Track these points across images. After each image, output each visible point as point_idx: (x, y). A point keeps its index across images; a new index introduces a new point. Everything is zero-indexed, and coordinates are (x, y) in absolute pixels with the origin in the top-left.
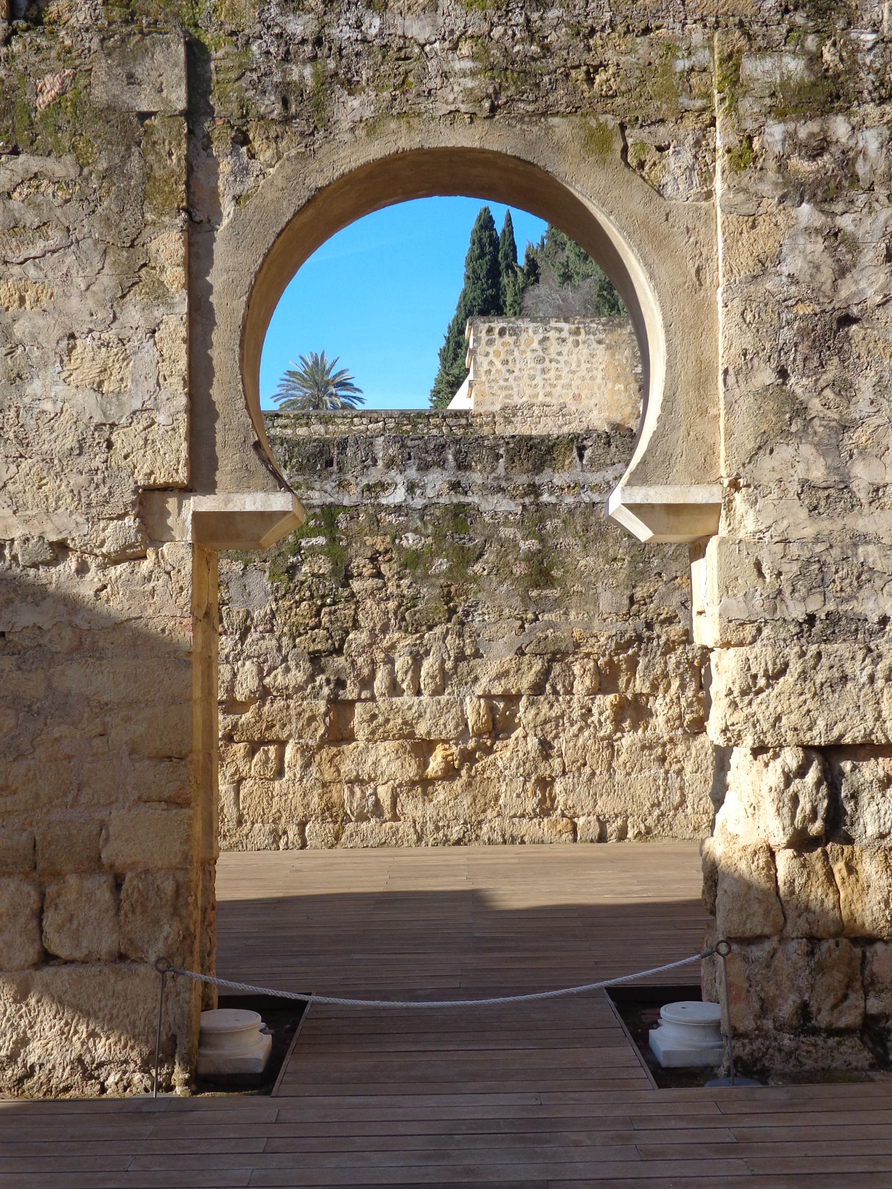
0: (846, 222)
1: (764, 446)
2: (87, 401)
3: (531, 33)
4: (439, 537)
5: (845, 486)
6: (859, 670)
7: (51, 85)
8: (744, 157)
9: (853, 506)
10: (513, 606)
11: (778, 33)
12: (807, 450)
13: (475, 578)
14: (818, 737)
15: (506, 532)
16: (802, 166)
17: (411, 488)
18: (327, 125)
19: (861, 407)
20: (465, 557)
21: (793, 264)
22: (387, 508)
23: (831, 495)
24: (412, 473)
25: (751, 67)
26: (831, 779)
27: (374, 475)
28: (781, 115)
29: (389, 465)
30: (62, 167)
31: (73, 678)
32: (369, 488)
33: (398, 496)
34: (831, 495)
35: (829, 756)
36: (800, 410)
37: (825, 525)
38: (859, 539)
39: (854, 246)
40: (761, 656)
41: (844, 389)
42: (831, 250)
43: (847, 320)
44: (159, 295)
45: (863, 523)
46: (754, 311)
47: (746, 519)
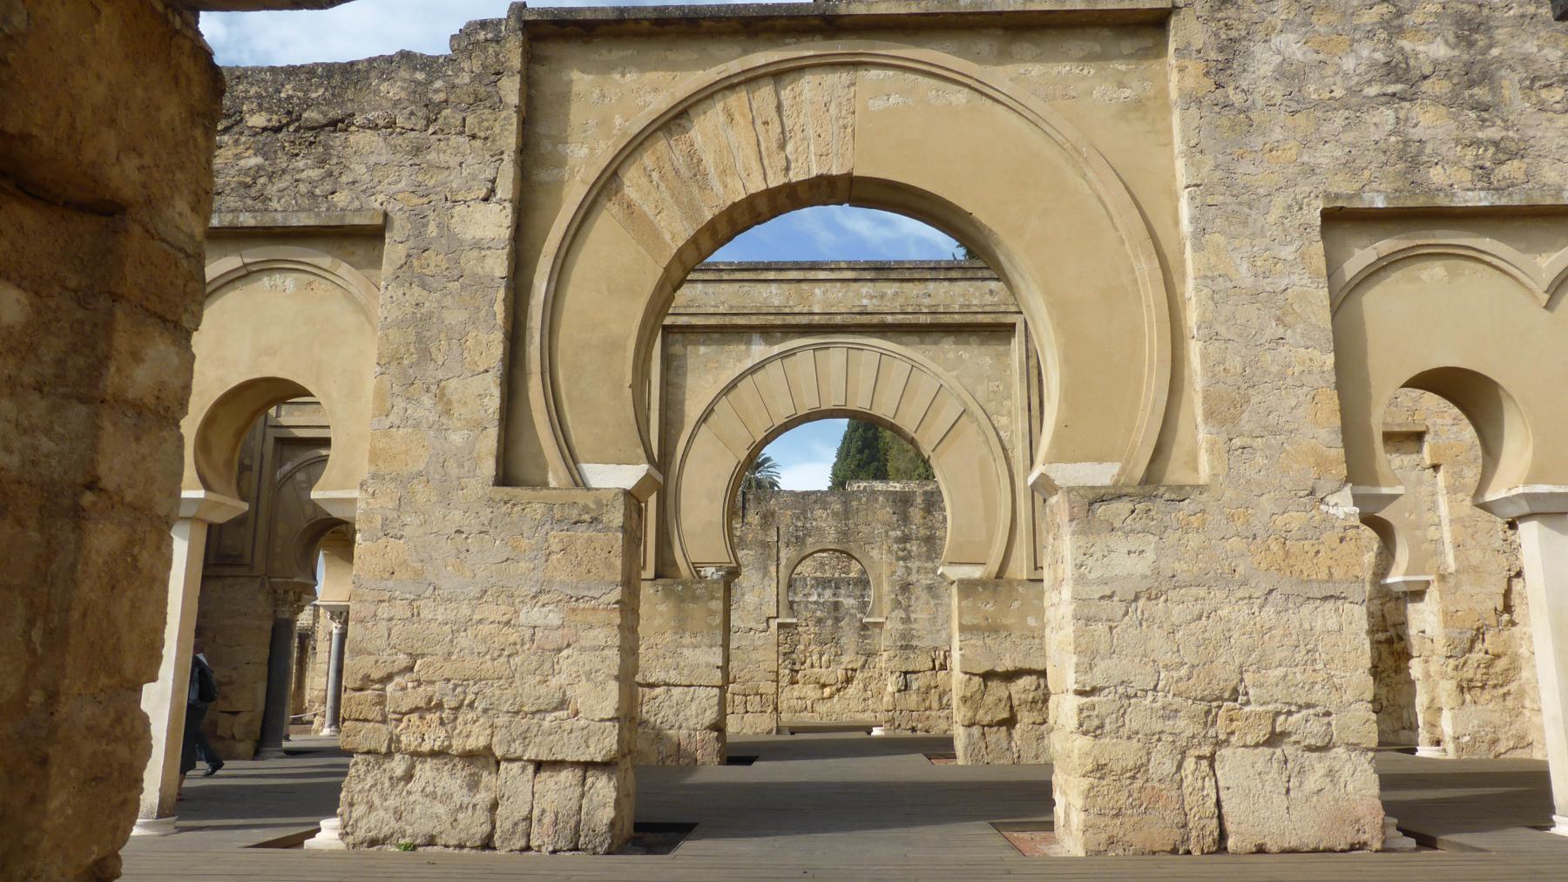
10: (855, 638)
16: (901, 554)
18: (804, 543)
20: (837, 620)
23: (906, 620)
31: (754, 656)
33: (814, 598)
34: (906, 620)
35: (906, 673)
40: (892, 653)
46: (892, 584)
47: (888, 626)
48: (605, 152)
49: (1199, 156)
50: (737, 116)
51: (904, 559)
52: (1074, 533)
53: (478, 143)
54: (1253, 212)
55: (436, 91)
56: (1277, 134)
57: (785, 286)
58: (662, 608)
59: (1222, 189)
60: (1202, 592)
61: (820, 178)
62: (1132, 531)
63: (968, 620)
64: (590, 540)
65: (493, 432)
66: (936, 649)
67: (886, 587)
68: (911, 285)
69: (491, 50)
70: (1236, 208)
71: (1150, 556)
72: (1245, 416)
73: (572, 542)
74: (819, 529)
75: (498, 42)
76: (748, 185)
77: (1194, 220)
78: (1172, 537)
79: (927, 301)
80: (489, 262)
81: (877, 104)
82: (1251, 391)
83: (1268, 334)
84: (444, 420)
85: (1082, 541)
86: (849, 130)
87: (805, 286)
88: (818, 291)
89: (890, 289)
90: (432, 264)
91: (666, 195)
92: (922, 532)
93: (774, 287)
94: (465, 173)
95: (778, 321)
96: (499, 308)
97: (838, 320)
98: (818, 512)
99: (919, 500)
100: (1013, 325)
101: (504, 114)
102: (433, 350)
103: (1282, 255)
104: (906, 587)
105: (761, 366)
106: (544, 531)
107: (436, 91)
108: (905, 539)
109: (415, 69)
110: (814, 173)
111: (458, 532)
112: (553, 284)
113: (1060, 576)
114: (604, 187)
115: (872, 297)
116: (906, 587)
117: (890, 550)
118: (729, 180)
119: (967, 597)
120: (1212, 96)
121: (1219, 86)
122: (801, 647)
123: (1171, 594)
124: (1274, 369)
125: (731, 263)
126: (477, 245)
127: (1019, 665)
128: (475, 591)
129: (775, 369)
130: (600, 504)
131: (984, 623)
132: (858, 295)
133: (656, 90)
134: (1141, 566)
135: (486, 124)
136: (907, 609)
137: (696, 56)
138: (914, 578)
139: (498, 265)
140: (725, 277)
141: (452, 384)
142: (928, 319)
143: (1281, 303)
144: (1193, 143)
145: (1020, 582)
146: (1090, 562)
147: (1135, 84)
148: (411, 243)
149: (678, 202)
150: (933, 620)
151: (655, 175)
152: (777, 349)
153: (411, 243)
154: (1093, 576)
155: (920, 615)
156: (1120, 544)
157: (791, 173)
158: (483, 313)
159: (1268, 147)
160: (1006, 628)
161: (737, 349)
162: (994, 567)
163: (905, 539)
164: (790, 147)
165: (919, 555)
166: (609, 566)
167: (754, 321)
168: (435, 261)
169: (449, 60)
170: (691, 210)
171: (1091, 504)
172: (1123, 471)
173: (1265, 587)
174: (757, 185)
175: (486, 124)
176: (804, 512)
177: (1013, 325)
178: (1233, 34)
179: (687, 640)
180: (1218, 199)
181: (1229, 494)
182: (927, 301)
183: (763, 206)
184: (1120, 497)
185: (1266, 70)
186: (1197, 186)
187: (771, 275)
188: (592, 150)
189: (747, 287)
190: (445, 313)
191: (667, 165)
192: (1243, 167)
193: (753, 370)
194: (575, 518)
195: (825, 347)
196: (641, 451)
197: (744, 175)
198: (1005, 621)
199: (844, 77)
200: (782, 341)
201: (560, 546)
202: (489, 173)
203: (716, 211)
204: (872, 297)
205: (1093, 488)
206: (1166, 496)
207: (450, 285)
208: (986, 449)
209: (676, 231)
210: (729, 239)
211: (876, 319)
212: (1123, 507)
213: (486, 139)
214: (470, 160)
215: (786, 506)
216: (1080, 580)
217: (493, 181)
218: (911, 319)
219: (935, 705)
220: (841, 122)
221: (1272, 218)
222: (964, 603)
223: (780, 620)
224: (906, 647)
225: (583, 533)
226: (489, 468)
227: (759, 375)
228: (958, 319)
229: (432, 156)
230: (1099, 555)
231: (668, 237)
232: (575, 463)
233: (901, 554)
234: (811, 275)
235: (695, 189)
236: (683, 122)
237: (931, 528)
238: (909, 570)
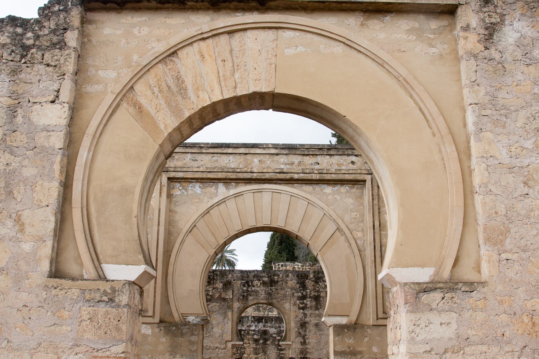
0: (306, 312)
1: (296, 338)
2: (220, 331)
3: (271, 290)
4: (261, 336)
7: (217, 295)
8: (295, 304)
9: (306, 344)
11: (298, 290)
13: (268, 344)
15: (274, 335)
17: (256, 326)
18: (247, 299)
19: (307, 333)
20: (266, 340)
22: (251, 331)
24: (256, 323)
25: (295, 294)
27: (249, 324)
28: (298, 299)
29: (252, 321)
30: (217, 304)
32: (248, 326)
33: (253, 328)
34: (304, 343)
36: (300, 333)
38: (307, 348)
41: (305, 331)
44: (228, 319)
45: (307, 347)
47: (294, 346)
48: (126, 75)
49: (476, 87)
50: (206, 56)
51: (303, 309)
52: (407, 312)
53: (50, 69)
54: (508, 120)
55: (28, 39)
56: (520, 77)
57: (238, 157)
58: (163, 340)
59: (490, 106)
60: (484, 348)
61: (255, 94)
62: (443, 310)
63: (339, 348)
64: (107, 313)
65: (49, 243)
67: (293, 324)
68: (308, 157)
69: (62, 16)
70: (499, 118)
71: (454, 326)
72: (508, 241)
73: (96, 314)
74: (257, 292)
75: (66, 12)
76: (212, 96)
77: (476, 124)
78: (467, 315)
79: (317, 167)
80: (53, 139)
81: (290, 52)
82: (510, 226)
83: (519, 193)
84: (19, 235)
85: (413, 316)
86: (273, 66)
87: (249, 157)
88: (256, 160)
89: (296, 159)
90: (18, 140)
91: (162, 102)
92: (313, 293)
93: (231, 157)
94: (41, 86)
95: (233, 176)
96: (57, 167)
97: (267, 176)
98: (256, 282)
99: (312, 276)
100: (365, 181)
101: (67, 52)
102: (15, 192)
103: (526, 145)
104: (303, 325)
105: (223, 201)
106: (78, 306)
107: (28, 39)
108: (303, 297)
109: (17, 26)
110: (251, 91)
111: (25, 306)
112: (91, 153)
113: (398, 337)
114: (124, 95)
115: (286, 164)
116: (303, 325)
117: (295, 304)
118: (200, 93)
119: (338, 335)
120: (483, 54)
121: (486, 48)
122: (245, 355)
123: (466, 349)
124: (523, 212)
125: (207, 144)
126: (47, 129)
128: (33, 344)
129: (231, 204)
130: (114, 290)
131: (348, 350)
132: (278, 162)
133: (158, 40)
134: (449, 332)
135: (56, 58)
136: (304, 337)
137: (183, 21)
138: (308, 319)
139: (57, 141)
140: (204, 151)
141: (26, 214)
142: (318, 177)
143: (526, 173)
144: (473, 80)
145: (369, 327)
146: (418, 330)
147: (439, 46)
148: (6, 128)
149: (169, 105)
150: (319, 342)
151: (156, 90)
152: (232, 192)
153: (6, 128)
154: (419, 339)
155: (312, 340)
156: (435, 318)
157: (238, 90)
158: (47, 170)
159: (515, 84)
160: (360, 353)
161: (211, 189)
163: (303, 297)
164: (237, 75)
165: (311, 307)
166: (118, 329)
167: (220, 175)
168: (20, 139)
169: (37, 21)
170: (176, 111)
171: (417, 294)
172: (437, 273)
173: (521, 344)
174: (217, 97)
175: (56, 58)
176: (247, 282)
177: (365, 181)
178: (493, 20)
180: (488, 112)
181: (500, 288)
182: (317, 167)
183: (220, 109)
184: (435, 289)
185: (511, 41)
186: (476, 104)
187: (230, 150)
188: (118, 74)
189: (216, 157)
190: (24, 170)
191: (164, 84)
192: (502, 94)
193: (218, 204)
194: (98, 298)
195: (260, 191)
196: (141, 257)
197: (209, 91)
198: (360, 349)
199: (271, 34)
200: (236, 187)
201: (88, 317)
202: (56, 87)
203: (193, 112)
204: (286, 164)
205: (419, 284)
206: (463, 289)
207: (28, 153)
208: (349, 251)
209: (168, 123)
210: (201, 129)
211: (288, 176)
212: (437, 296)
213: (55, 66)
214: (44, 78)
215: (238, 279)
216: (412, 341)
217: (58, 91)
218: (308, 176)
220: (268, 61)
221: (519, 124)
222: (337, 339)
223: (233, 343)
225: (102, 309)
226: (45, 266)
227: (223, 206)
228: (334, 177)
229: (23, 76)
230: (423, 325)
231: (162, 127)
232: (100, 263)
233: (301, 306)
234: (253, 151)
235: (179, 98)
236: (174, 59)
237: (318, 291)
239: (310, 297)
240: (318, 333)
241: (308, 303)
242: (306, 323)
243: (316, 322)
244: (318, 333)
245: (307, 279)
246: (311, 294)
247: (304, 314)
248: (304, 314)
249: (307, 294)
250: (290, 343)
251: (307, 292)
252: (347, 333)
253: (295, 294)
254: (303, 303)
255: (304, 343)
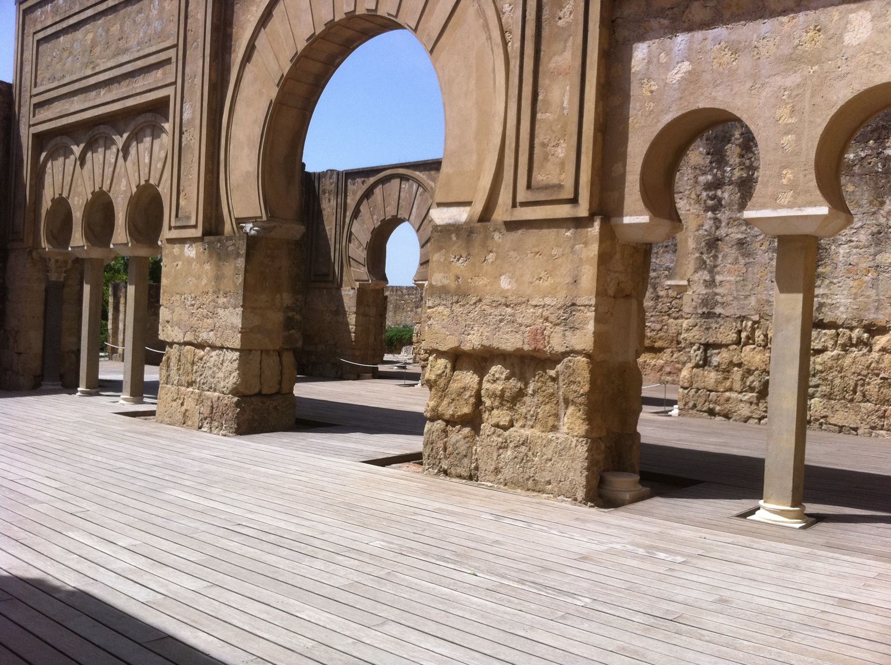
1: (696, 272)
5: (714, 281)
6: (714, 326)
9: (715, 286)
12: (706, 272)
14: (703, 341)
16: (710, 203)
21: (706, 227)
26: (705, 351)
28: (705, 189)
34: (711, 283)
35: (707, 346)
36: (705, 262)
37: (709, 291)
38: (716, 294)
39: (720, 221)
40: (691, 321)
41: (715, 257)
42: (714, 223)
43: (718, 240)
45: (717, 290)
46: (697, 240)
51: (714, 209)
58: (207, 267)
66: (743, 318)
92: (737, 174)
104: (713, 244)
108: (717, 184)
116: (713, 244)
117: (698, 200)
127: (486, 343)
136: (712, 271)
138: (722, 232)
162: (478, 207)
163: (717, 184)
165: (730, 204)
179: (222, 300)
219: (737, 386)
224: (709, 315)
233: (710, 203)
238: (717, 222)
239: (731, 183)
240: (742, 261)
241: (726, 195)
242: (718, 240)
243: (740, 236)
244: (742, 261)
245: (729, 141)
246: (732, 174)
247: (716, 219)
248: (716, 219)
249: (724, 177)
250: (685, 283)
251: (725, 171)
252: (455, 243)
253: (702, 179)
254: (712, 198)
255: (711, 283)
